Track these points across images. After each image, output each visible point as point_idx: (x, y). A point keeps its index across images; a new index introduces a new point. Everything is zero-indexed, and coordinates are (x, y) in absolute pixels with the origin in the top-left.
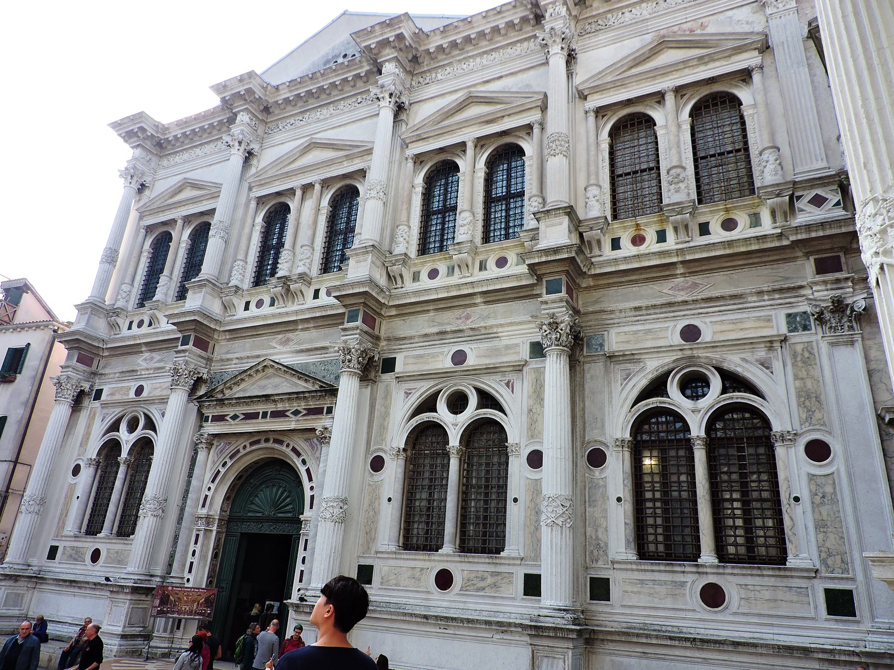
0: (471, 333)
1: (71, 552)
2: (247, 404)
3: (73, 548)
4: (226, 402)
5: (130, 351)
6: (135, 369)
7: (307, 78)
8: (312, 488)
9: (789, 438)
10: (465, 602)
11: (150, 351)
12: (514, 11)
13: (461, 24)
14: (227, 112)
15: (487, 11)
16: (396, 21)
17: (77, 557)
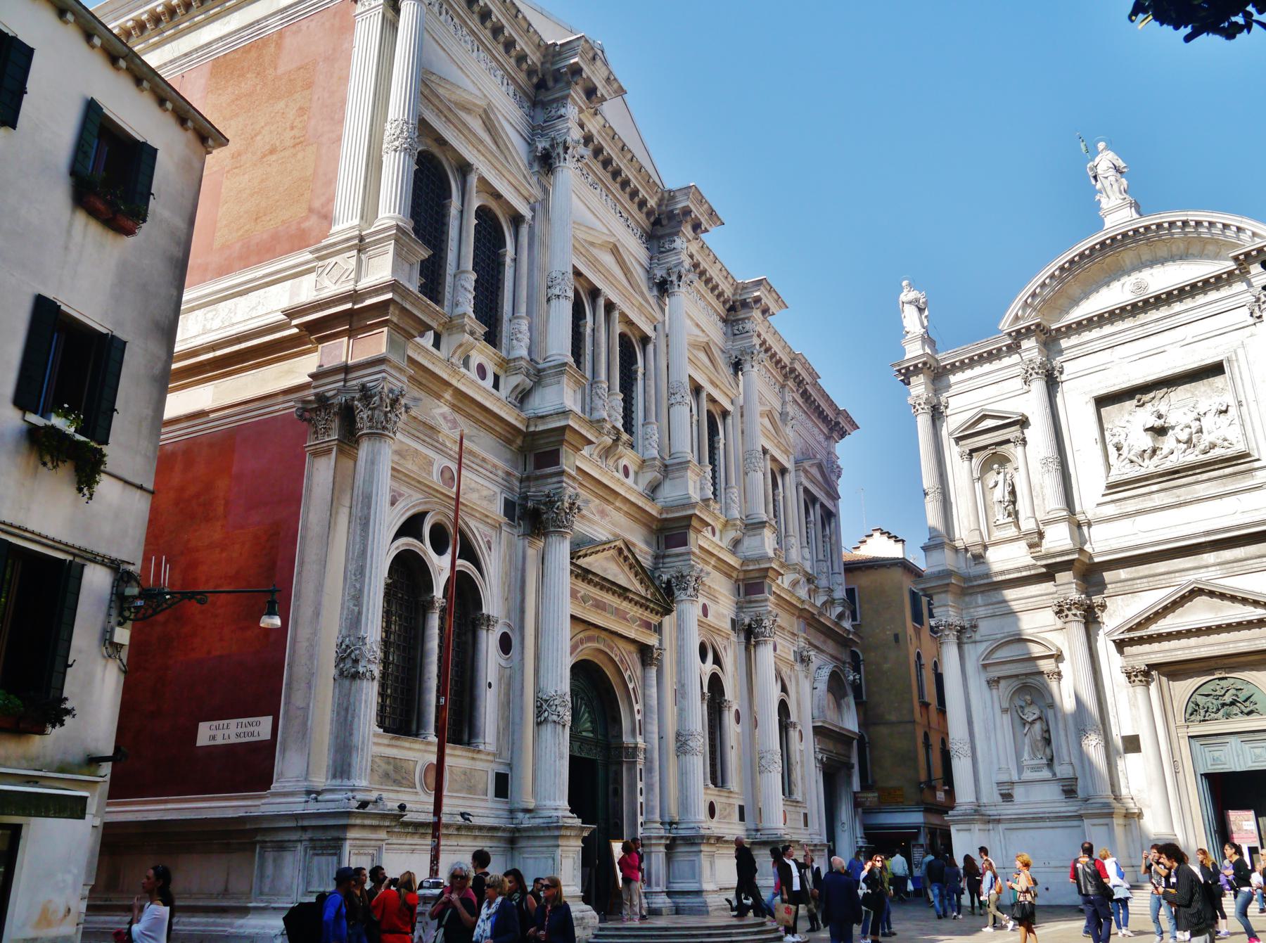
0: (708, 590)
1: (384, 766)
2: (603, 588)
3: (388, 760)
4: (590, 576)
5: (424, 381)
6: (432, 423)
7: (621, 145)
8: (638, 711)
9: (794, 725)
10: (720, 828)
11: (454, 407)
12: (729, 286)
13: (712, 256)
14: (538, 54)
15: (726, 270)
16: (715, 219)
17: (399, 778)
